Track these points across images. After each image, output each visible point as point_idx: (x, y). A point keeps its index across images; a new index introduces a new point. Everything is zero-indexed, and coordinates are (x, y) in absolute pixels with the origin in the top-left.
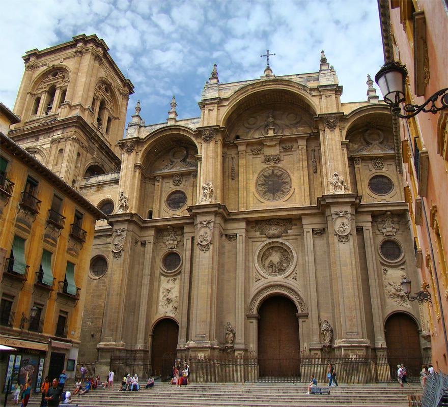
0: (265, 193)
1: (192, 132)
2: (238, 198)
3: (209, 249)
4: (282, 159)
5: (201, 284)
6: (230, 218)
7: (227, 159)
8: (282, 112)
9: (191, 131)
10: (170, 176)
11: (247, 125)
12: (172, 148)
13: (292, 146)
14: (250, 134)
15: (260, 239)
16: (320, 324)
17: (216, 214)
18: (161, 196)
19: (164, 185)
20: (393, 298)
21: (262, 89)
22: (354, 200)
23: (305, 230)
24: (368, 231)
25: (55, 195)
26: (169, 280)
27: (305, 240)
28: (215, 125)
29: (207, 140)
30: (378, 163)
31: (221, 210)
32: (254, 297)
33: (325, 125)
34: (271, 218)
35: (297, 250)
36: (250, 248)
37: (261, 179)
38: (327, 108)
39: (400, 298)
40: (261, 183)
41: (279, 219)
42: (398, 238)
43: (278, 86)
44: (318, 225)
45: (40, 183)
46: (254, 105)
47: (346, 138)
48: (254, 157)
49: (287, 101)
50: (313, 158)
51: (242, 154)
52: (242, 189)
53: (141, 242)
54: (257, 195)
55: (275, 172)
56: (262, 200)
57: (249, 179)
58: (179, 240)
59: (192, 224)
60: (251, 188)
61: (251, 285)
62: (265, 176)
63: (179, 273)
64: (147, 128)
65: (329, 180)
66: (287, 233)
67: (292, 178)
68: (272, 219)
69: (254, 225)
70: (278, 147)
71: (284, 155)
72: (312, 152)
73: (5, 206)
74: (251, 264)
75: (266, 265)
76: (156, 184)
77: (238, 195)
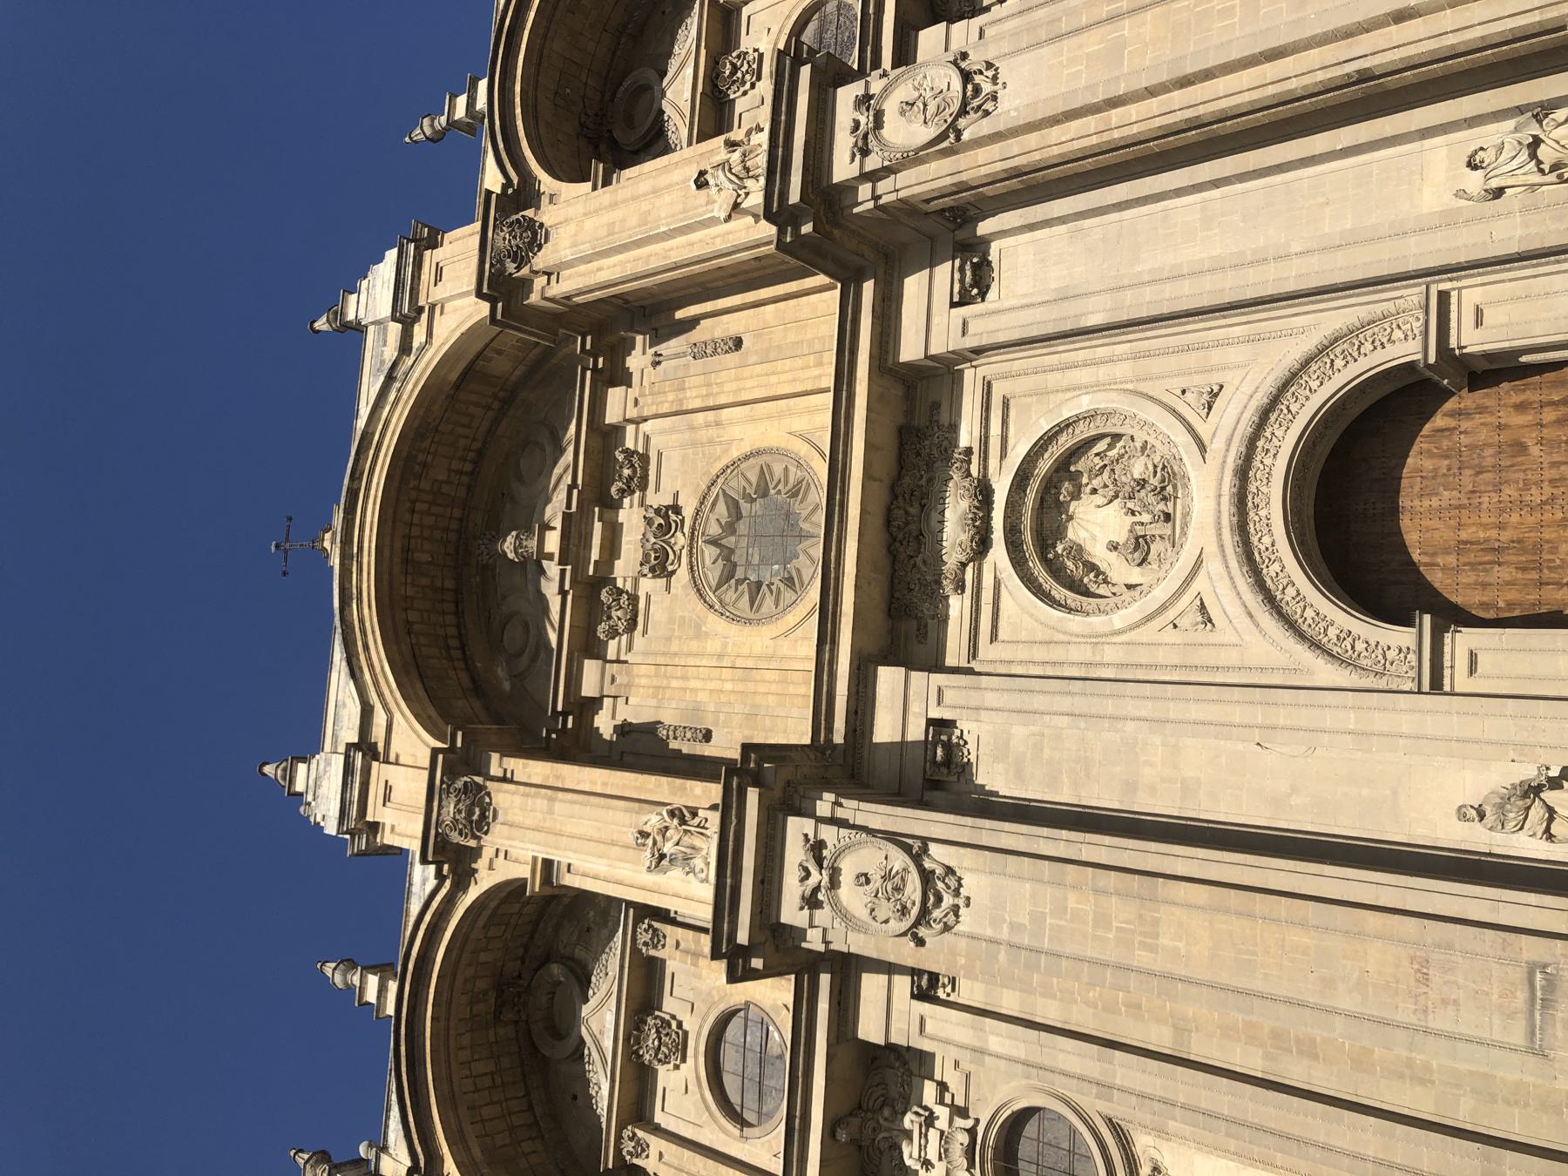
1: (444, 891)
3: (950, 871)
4: (669, 501)
5: (1152, 949)
8: (508, 506)
9: (439, 898)
11: (525, 659)
21: (369, 559)
22: (805, 72)
23: (957, 343)
24: (988, 32)
29: (480, 818)
30: (735, 69)
32: (1301, 635)
33: (525, 271)
35: (1061, 396)
36: (1022, 653)
40: (746, 597)
41: (892, 489)
43: (373, 492)
46: (450, 619)
48: (640, 627)
51: (613, 679)
52: (751, 686)
54: (791, 618)
55: (714, 530)
57: (720, 656)
60: (758, 650)
61: (1229, 657)
65: (723, 215)
66: (969, 451)
67: (746, 448)
68: (888, 523)
69: (914, 624)
71: (657, 489)
74: (1110, 654)
75: (1136, 575)
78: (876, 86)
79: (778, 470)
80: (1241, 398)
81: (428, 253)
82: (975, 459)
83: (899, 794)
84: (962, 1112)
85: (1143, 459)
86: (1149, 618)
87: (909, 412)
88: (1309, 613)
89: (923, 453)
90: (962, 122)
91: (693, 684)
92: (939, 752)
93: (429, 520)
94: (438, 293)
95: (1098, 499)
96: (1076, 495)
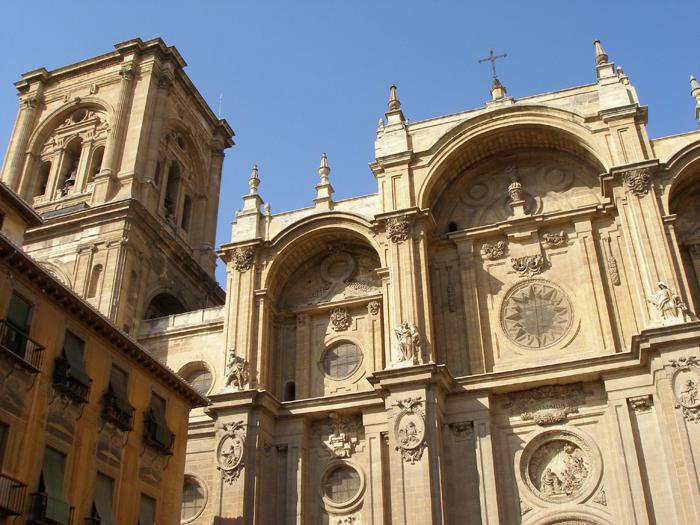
0: (521, 333)
2: (467, 348)
6: (457, 390)
7: (437, 272)
8: (534, 169)
9: (363, 222)
10: (327, 313)
11: (469, 201)
12: (326, 256)
13: (565, 237)
14: (477, 217)
17: (428, 385)
18: (311, 352)
19: (315, 331)
25: (114, 365)
26: (340, 522)
28: (409, 207)
31: (440, 377)
34: (543, 384)
37: (509, 307)
38: (625, 153)
40: (510, 313)
44: (639, 390)
45: (87, 343)
46: (478, 158)
47: (671, 213)
48: (491, 262)
49: (541, 146)
50: (608, 254)
53: (277, 448)
58: (354, 440)
59: (381, 407)
62: (516, 300)
63: (359, 507)
64: (274, 220)
65: (648, 298)
66: (577, 412)
67: (573, 299)
68: (543, 386)
71: (551, 255)
72: (606, 244)
73: (28, 390)
76: (299, 329)
77: (467, 341)
79: (566, 317)
80: (601, 514)
81: (632, 120)
82: (575, 415)
83: (445, 415)
84: (350, 454)
87: (589, 383)
90: (682, 408)
91: (471, 301)
92: (462, 428)
93: (518, 137)
94: (613, 132)
96: (567, 452)
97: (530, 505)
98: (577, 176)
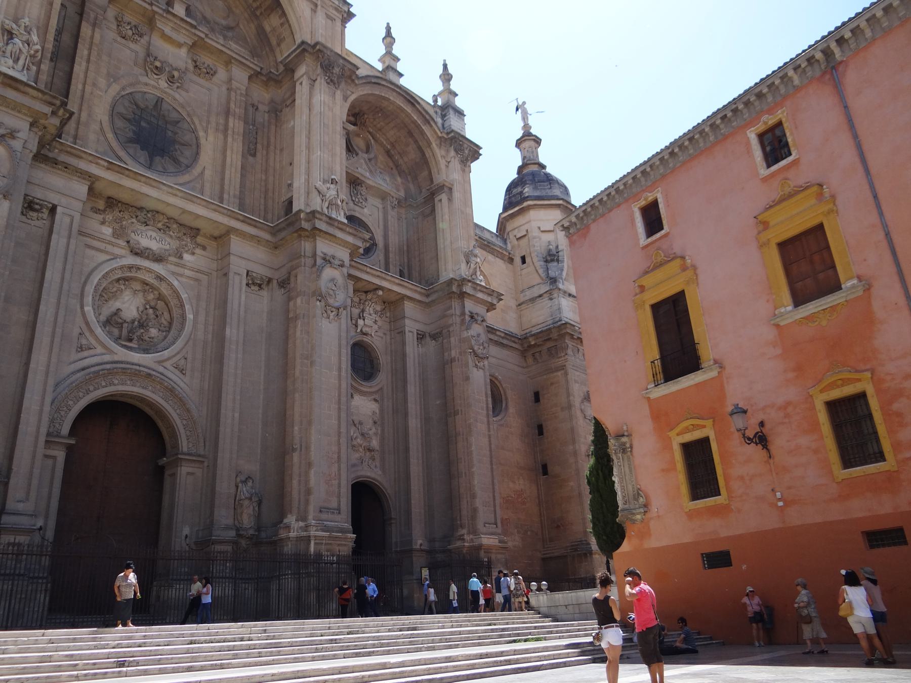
0: (131, 141)
6: (51, 155)
15: (109, 248)
16: (237, 487)
20: (357, 451)
23: (233, 268)
27: (230, 289)
34: (160, 207)
39: (368, 453)
40: (125, 112)
42: (378, 341)
48: (119, 39)
54: (110, 136)
56: (122, 153)
57: (94, 85)
62: (136, 105)
65: (317, 186)
66: (181, 257)
67: (202, 141)
69: (102, 208)
70: (183, 52)
72: (251, 109)
75: (103, 318)
78: (345, 270)
79: (188, 153)
85: (157, 334)
86: (87, 323)
88: (81, 394)
89: (184, 237)
90: (323, 303)
92: (37, 207)
95: (141, 309)
97: (93, 342)
98: (242, 27)
